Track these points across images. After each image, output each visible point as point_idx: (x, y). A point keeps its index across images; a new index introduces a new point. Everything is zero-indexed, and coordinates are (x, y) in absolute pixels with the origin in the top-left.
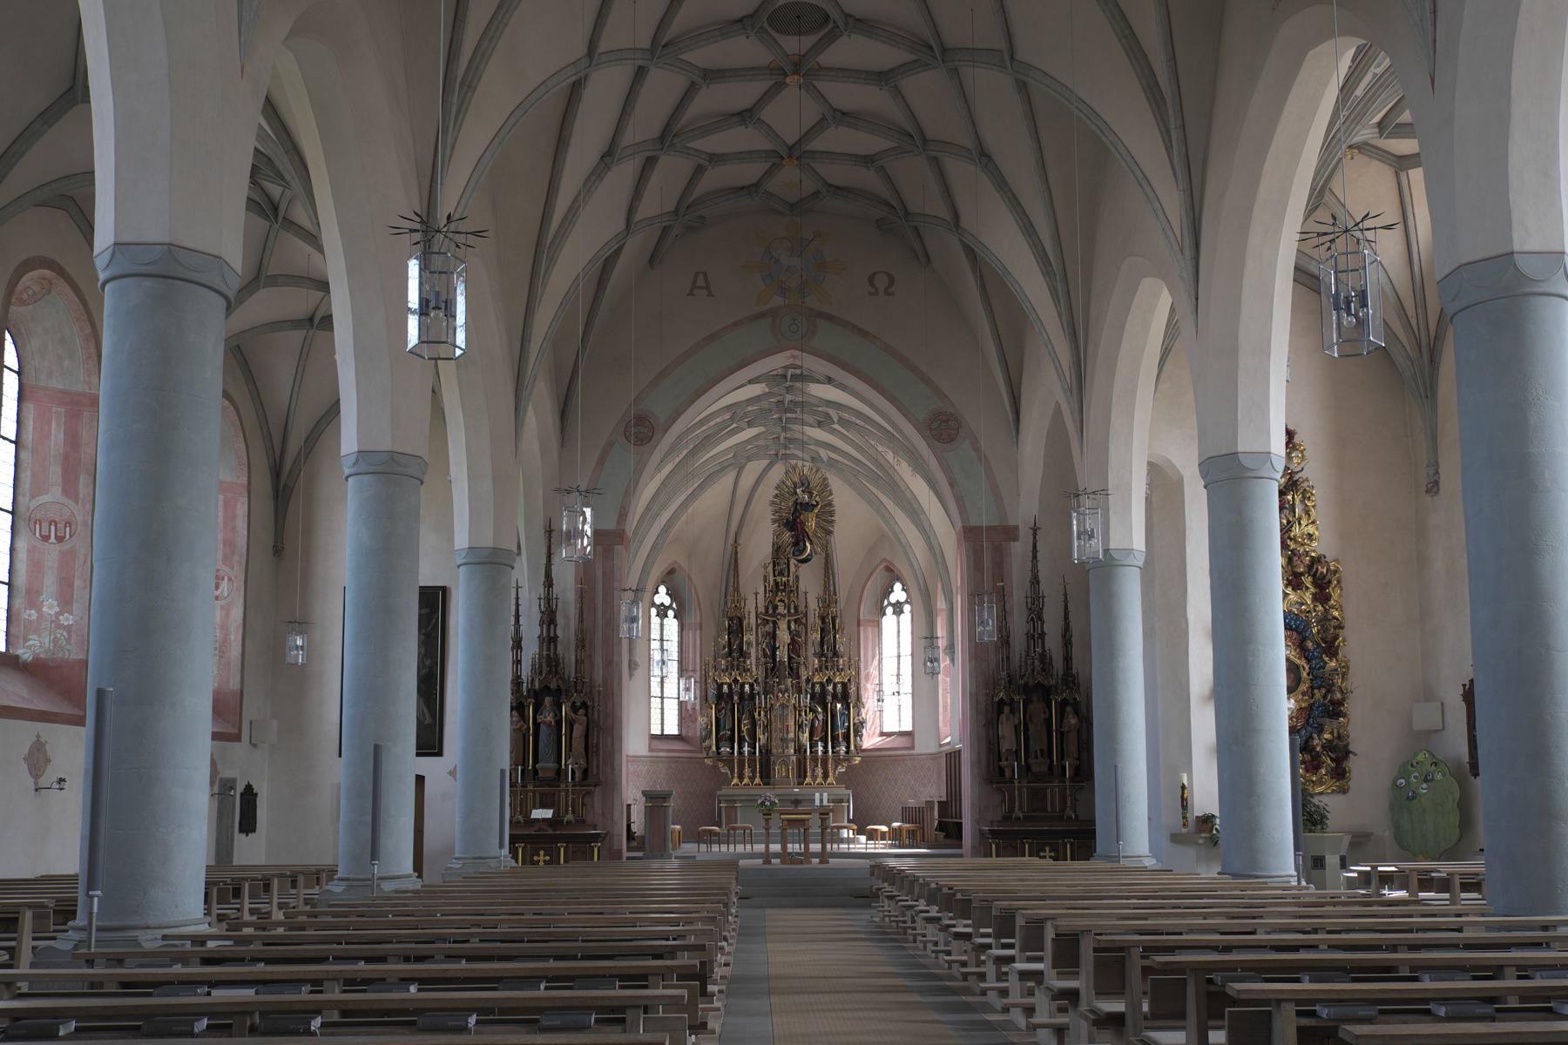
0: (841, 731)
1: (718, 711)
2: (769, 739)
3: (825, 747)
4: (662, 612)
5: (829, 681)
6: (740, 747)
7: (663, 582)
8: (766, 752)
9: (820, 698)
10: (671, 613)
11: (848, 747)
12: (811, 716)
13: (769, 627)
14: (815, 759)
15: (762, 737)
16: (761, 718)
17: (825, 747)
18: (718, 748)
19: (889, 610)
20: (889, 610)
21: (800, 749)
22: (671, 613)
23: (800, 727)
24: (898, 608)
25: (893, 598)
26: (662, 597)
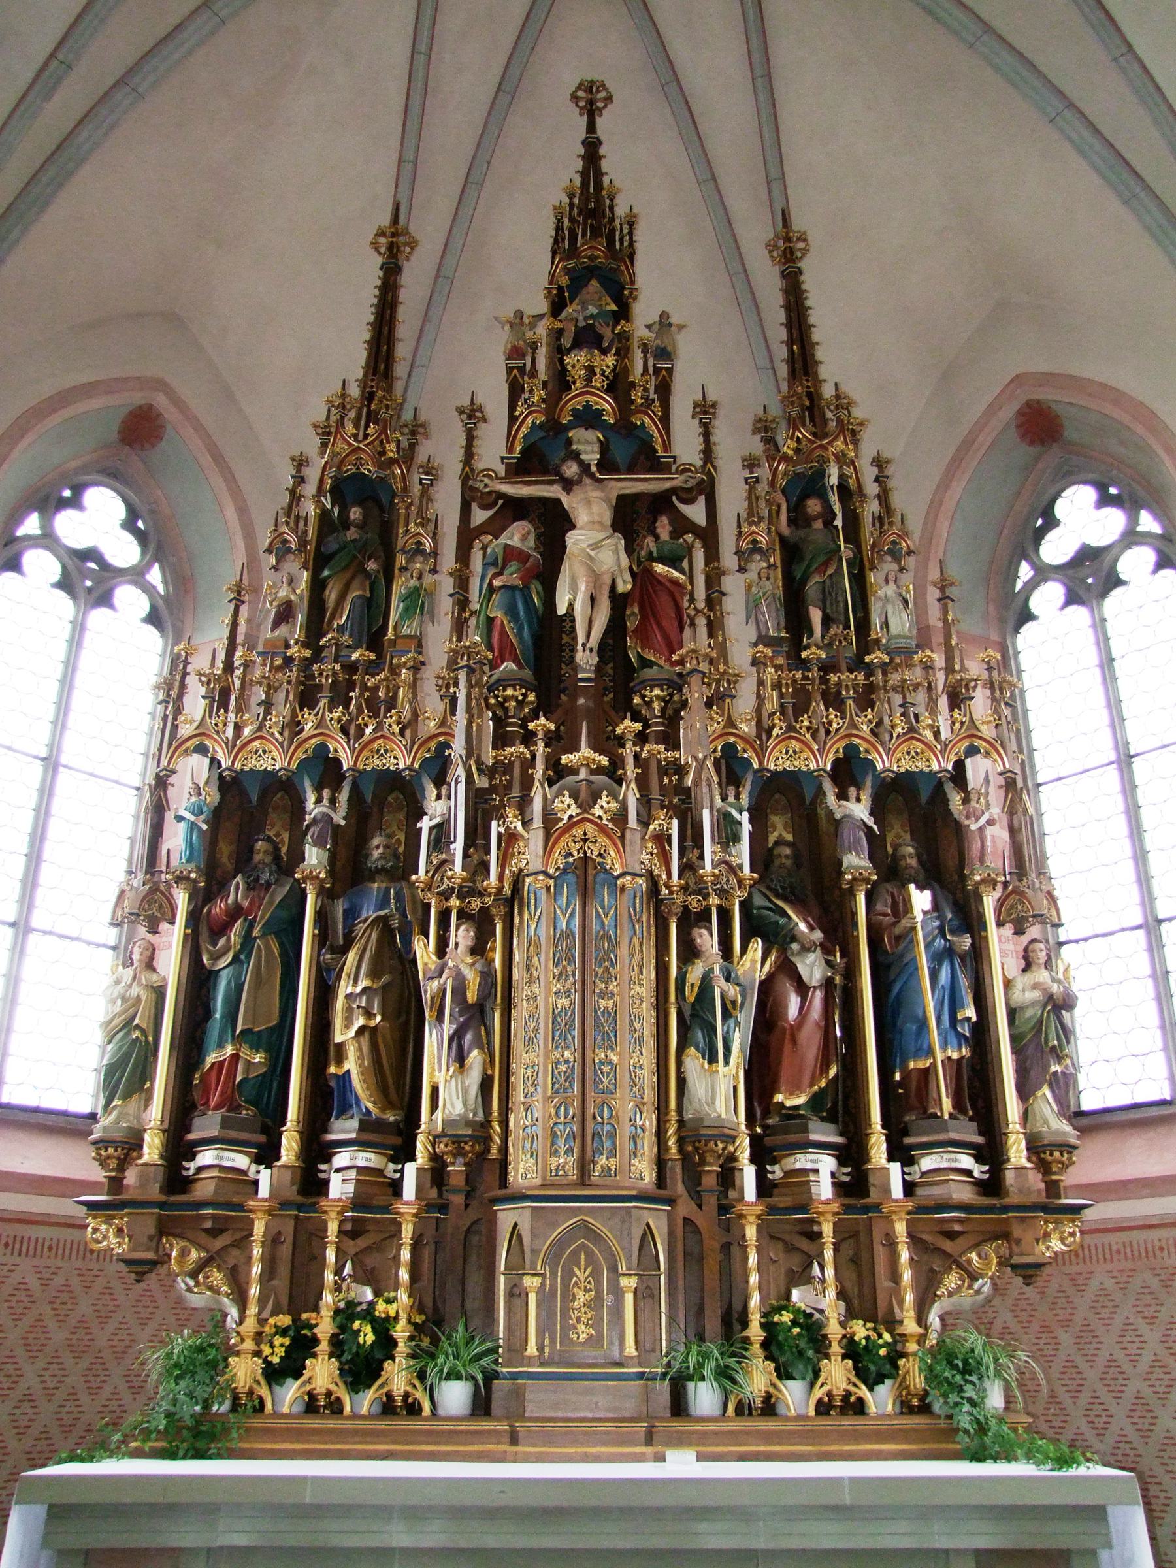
0: (943, 1052)
1: (202, 930)
2: (496, 1087)
3: (852, 1153)
4: (86, 578)
5: (849, 770)
6: (317, 1150)
7: (114, 476)
8: (478, 1160)
9: (802, 875)
10: (131, 601)
11: (991, 1151)
12: (754, 962)
13: (519, 535)
14: (793, 1235)
15: (449, 1090)
16: (443, 964)
17: (852, 1153)
18: (179, 1147)
19: (1047, 598)
20: (1047, 598)
21: (690, 1155)
22: (131, 601)
23: (695, 1020)
24: (1090, 577)
25: (1056, 548)
26: (99, 520)
